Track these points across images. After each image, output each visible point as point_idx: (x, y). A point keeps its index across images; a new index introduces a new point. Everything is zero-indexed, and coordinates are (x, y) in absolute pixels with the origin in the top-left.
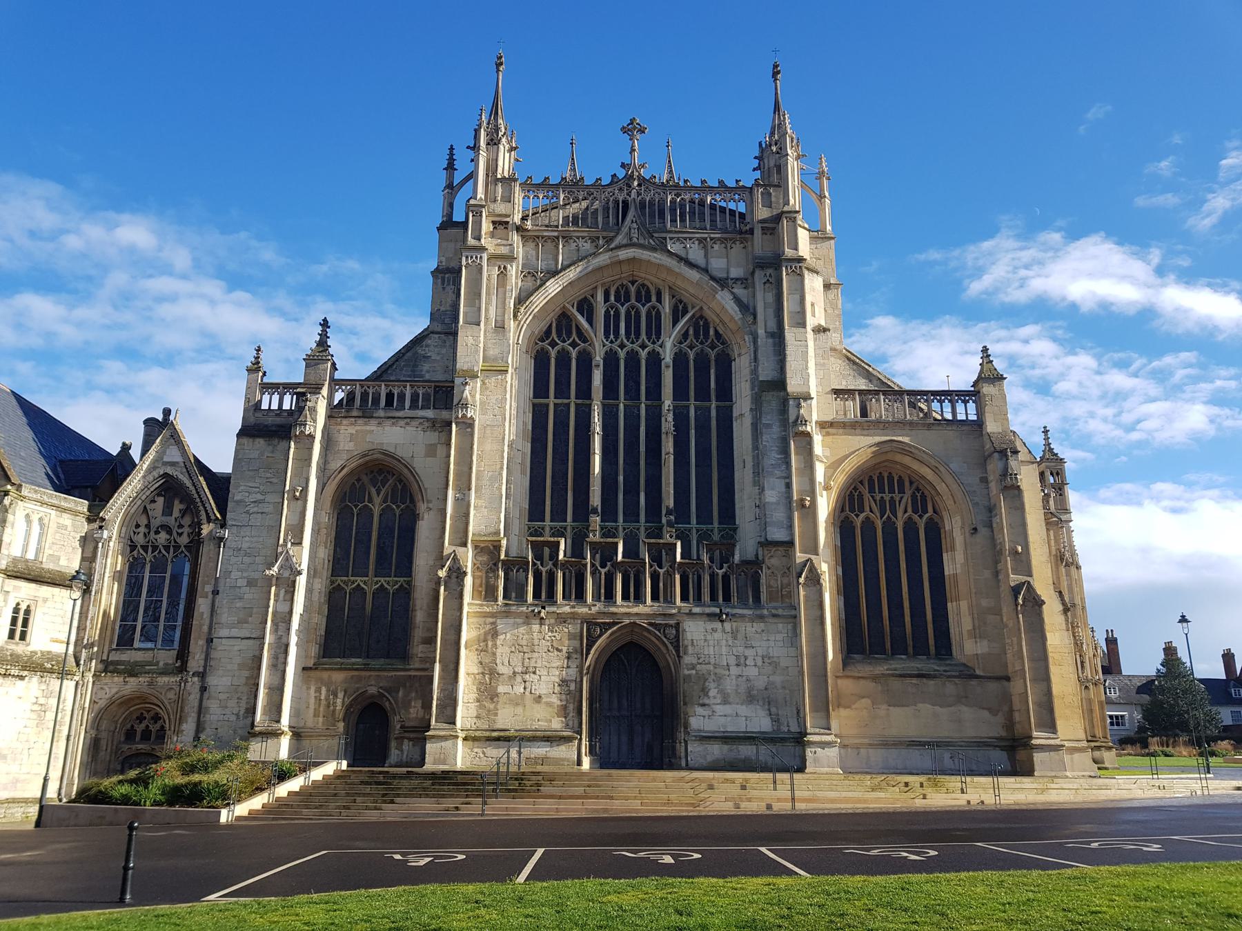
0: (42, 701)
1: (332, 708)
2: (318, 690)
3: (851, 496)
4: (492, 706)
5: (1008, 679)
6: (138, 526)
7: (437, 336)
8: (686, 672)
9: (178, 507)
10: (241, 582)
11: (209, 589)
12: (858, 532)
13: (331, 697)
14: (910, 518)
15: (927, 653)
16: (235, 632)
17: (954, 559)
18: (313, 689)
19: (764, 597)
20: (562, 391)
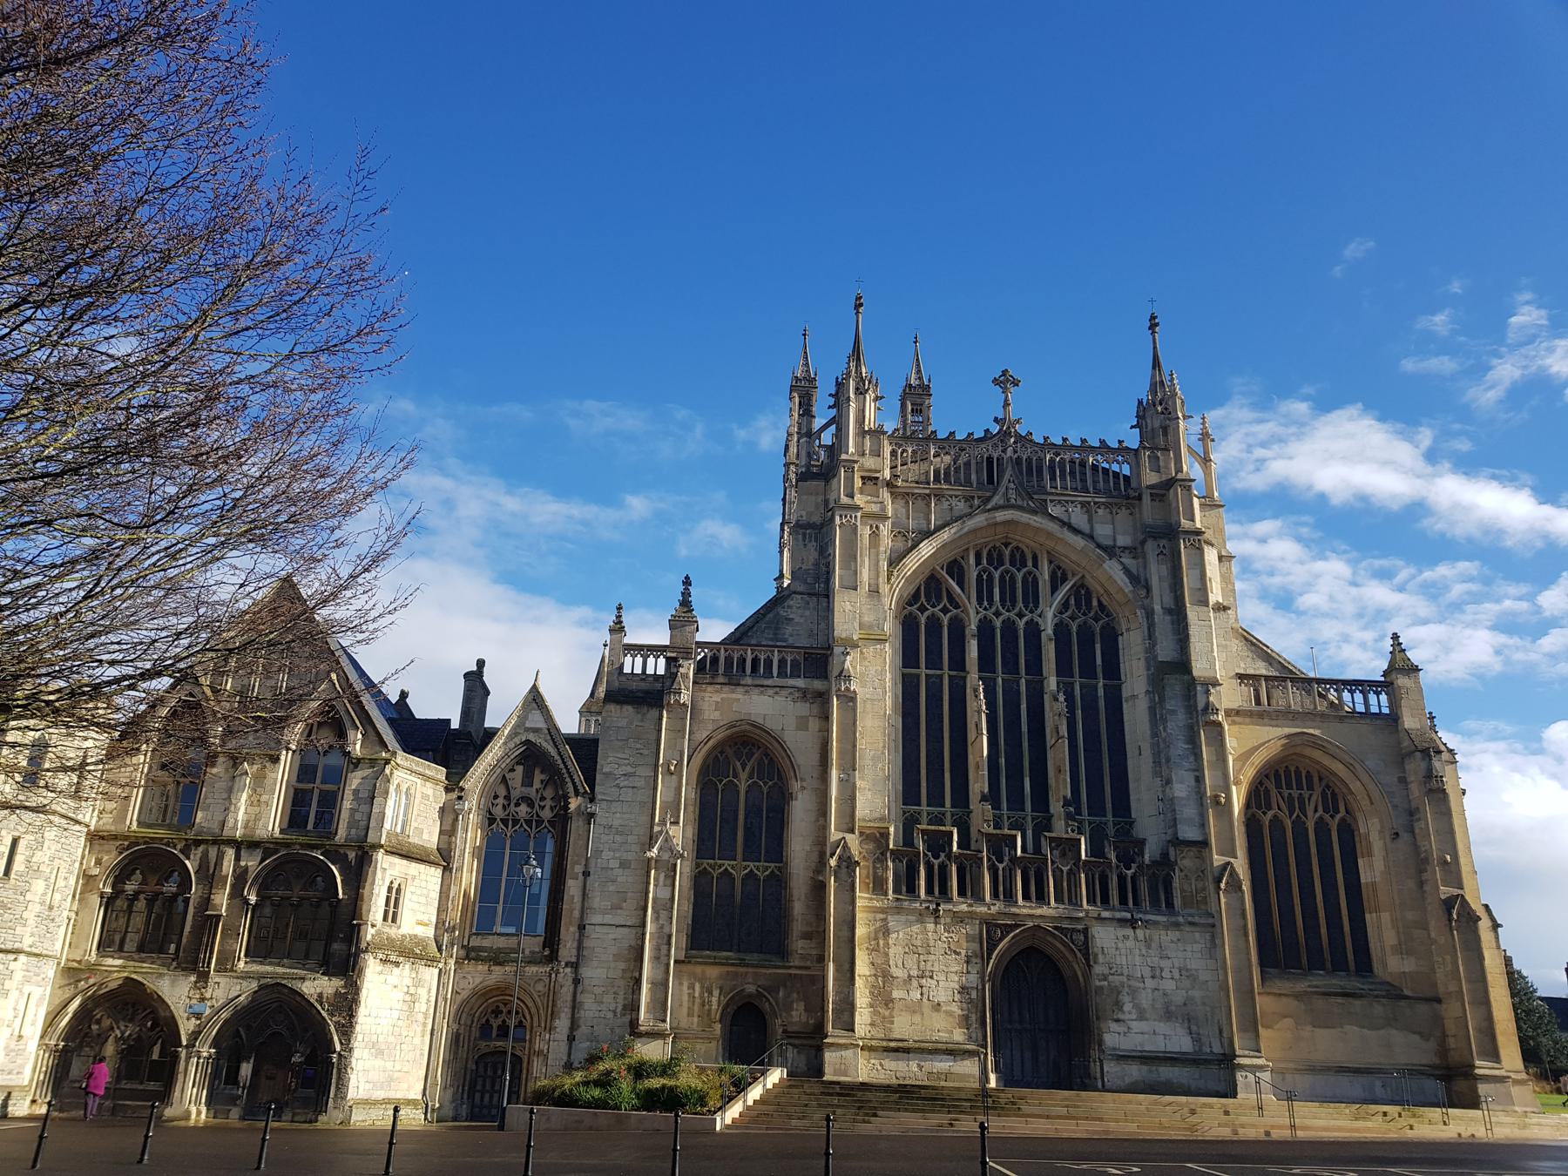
0: (412, 991)
1: (707, 1007)
2: (692, 987)
4: (887, 1013)
5: (1439, 1001)
6: (496, 797)
7: (799, 597)
8: (1098, 983)
9: (538, 777)
10: (614, 864)
11: (579, 869)
12: (1266, 832)
13: (706, 995)
14: (1321, 818)
15: (1347, 970)
16: (608, 919)
17: (1371, 866)
18: (686, 984)
19: (1177, 902)
20: (934, 661)
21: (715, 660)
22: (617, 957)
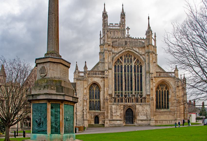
2: (90, 115)
3: (158, 87)
17: (170, 96)
19: (146, 102)
21: (90, 73)
22: (81, 111)
